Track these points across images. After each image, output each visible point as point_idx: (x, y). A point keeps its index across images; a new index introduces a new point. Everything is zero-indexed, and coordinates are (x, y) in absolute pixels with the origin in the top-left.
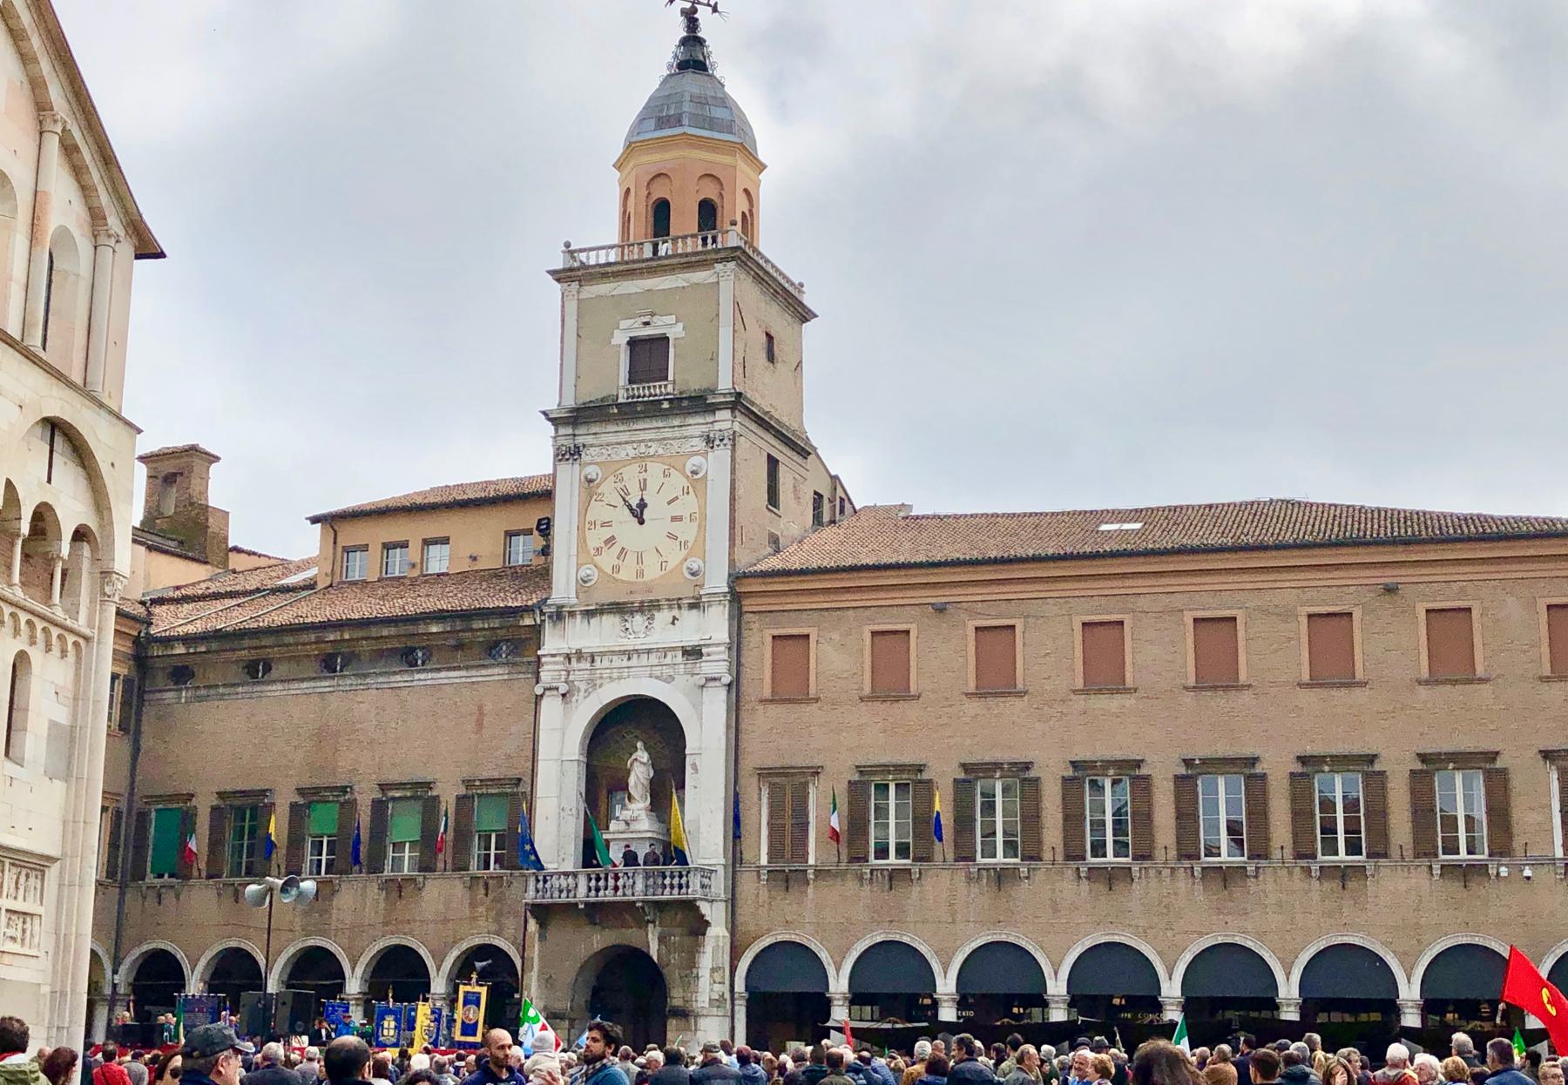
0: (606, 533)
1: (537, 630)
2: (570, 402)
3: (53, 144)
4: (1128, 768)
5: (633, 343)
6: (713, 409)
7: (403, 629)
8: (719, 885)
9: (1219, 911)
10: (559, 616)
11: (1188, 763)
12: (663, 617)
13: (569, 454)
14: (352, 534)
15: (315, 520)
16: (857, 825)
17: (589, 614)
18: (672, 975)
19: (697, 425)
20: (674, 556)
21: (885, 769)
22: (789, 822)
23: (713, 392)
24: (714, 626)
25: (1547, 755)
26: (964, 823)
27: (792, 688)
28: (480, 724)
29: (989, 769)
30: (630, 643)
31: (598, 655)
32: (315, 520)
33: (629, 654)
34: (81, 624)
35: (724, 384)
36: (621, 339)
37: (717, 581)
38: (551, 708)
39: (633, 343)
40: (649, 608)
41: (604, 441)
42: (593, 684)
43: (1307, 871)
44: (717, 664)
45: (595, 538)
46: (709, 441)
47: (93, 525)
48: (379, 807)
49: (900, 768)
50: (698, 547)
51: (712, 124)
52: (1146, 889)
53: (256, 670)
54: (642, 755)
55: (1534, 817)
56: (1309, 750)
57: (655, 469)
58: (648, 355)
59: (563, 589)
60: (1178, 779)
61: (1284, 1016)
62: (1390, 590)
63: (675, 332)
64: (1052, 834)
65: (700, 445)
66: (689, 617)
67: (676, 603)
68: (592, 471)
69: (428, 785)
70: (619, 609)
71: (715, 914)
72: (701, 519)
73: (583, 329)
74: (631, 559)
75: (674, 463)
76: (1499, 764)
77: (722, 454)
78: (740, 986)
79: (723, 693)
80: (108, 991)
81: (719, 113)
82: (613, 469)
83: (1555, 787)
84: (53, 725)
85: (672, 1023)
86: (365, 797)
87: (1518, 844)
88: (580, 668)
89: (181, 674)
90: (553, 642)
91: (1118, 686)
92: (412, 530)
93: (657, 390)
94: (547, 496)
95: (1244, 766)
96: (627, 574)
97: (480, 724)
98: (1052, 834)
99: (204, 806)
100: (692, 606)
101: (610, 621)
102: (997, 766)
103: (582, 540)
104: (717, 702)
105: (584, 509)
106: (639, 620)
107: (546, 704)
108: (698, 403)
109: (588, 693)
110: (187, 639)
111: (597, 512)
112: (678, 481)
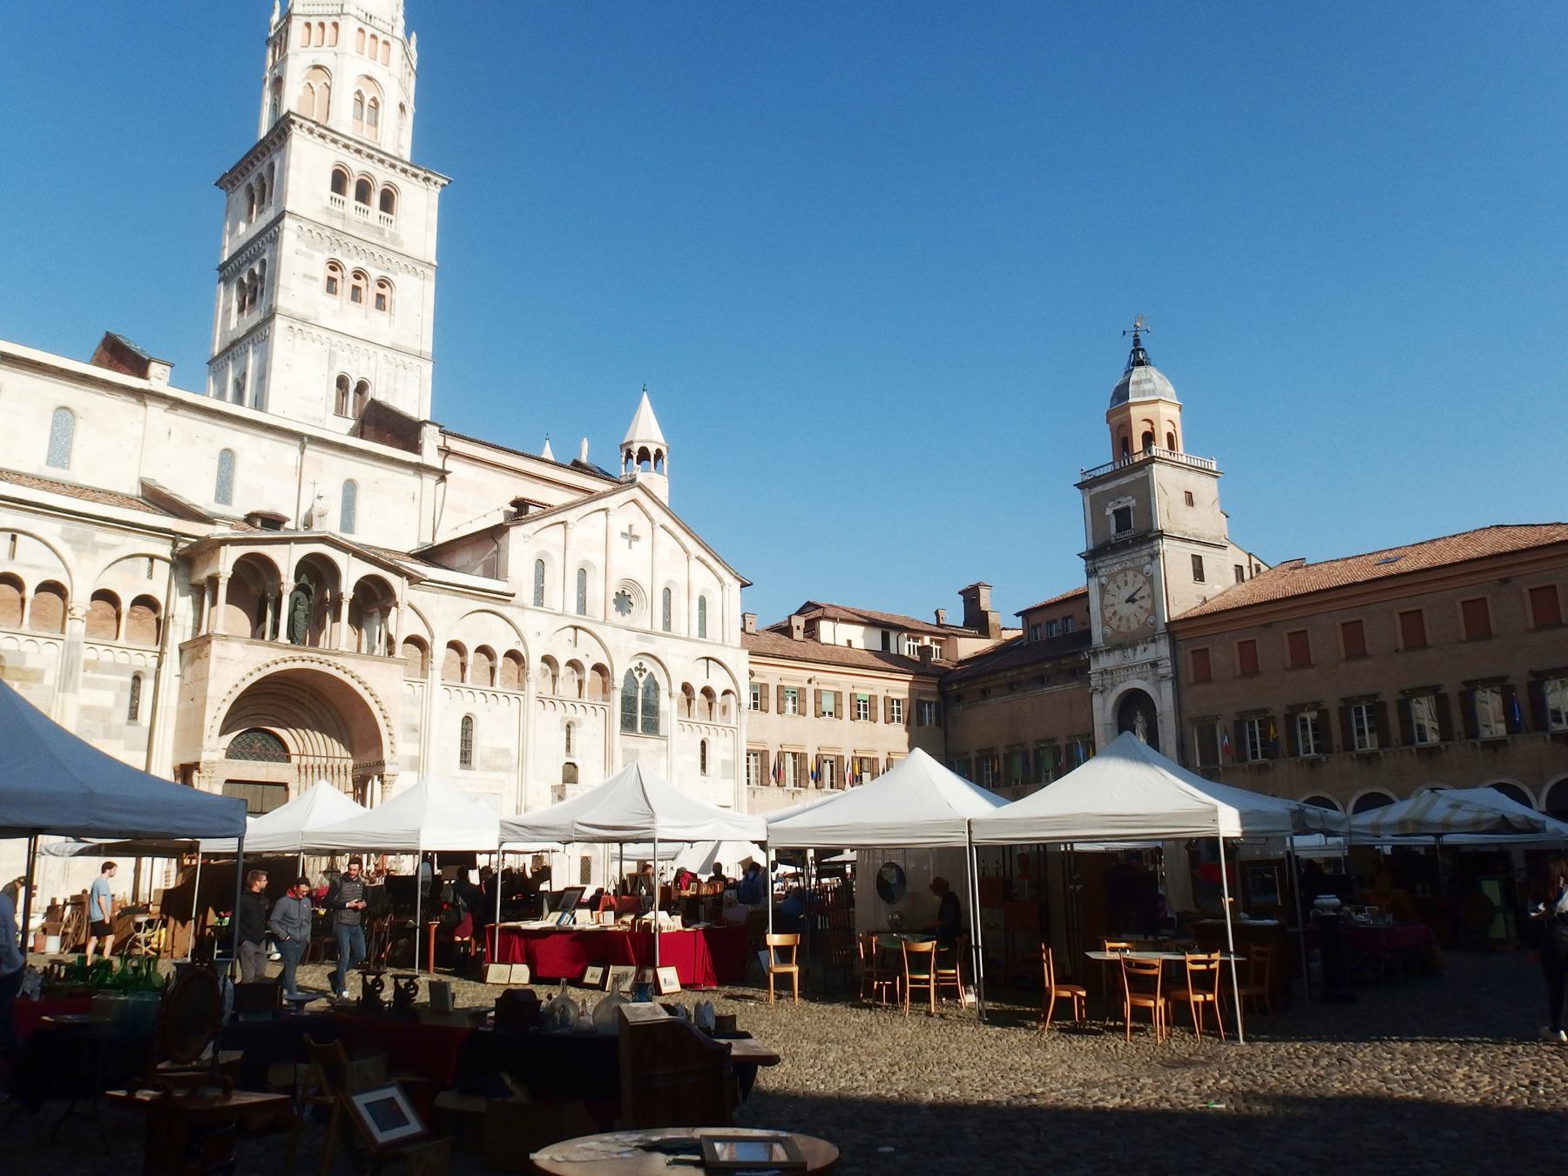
0: (1112, 610)
2: (1091, 547)
3: (695, 563)
4: (1316, 705)
5: (1115, 512)
10: (1096, 654)
11: (1403, 692)
12: (1140, 648)
13: (1091, 573)
14: (1035, 619)
15: (1017, 615)
16: (1239, 740)
17: (1108, 651)
20: (1143, 617)
21: (1250, 712)
23: (1151, 531)
24: (1163, 649)
26: (1292, 736)
27: (1203, 675)
29: (1303, 707)
30: (1128, 662)
32: (1017, 615)
33: (1127, 669)
34: (733, 724)
36: (1109, 512)
38: (1097, 700)
39: (1115, 512)
40: (1133, 645)
41: (1110, 565)
42: (1113, 685)
43: (1474, 745)
44: (1166, 668)
45: (1108, 614)
47: (733, 688)
48: (1036, 752)
49: (1257, 712)
51: (1144, 393)
53: (985, 693)
54: (1140, 718)
56: (1469, 677)
57: (1130, 574)
58: (1122, 516)
60: (1399, 702)
62: (1504, 581)
63: (1132, 503)
64: (1337, 739)
65: (1147, 559)
66: (1152, 647)
68: (1104, 580)
69: (1053, 740)
70: (1121, 647)
73: (1096, 509)
74: (1124, 621)
75: (1139, 570)
79: (1170, 684)
81: (1147, 386)
82: (1112, 577)
84: (724, 761)
86: (1031, 747)
88: (1108, 680)
89: (959, 698)
90: (1094, 667)
91: (1363, 655)
92: (1057, 614)
93: (1127, 533)
94: (1085, 595)
95: (1434, 691)
98: (1337, 739)
99: (973, 756)
100: (1154, 641)
101: (1118, 653)
102: (1305, 705)
105: (1102, 599)
107: (1095, 697)
111: (1109, 599)
112: (1141, 578)
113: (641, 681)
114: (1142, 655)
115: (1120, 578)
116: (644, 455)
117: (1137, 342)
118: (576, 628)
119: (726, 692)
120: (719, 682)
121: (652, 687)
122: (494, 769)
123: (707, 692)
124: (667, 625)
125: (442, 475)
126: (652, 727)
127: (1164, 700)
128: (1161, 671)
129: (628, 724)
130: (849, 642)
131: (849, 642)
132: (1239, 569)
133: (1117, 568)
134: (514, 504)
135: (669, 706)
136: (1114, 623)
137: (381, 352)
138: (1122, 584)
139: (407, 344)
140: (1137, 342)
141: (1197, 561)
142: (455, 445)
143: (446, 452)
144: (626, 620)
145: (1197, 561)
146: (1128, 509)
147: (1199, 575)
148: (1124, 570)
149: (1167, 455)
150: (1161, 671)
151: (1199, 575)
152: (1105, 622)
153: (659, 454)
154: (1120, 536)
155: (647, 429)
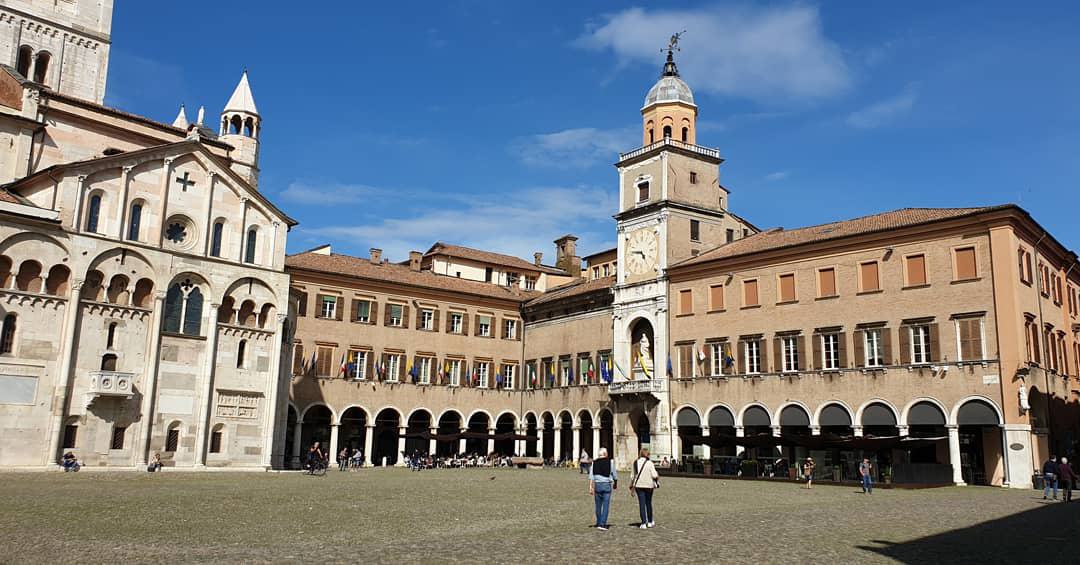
1: (613, 296)
6: (661, 207)
7: (581, 298)
8: (664, 386)
9: (830, 390)
10: (618, 289)
18: (650, 419)
19: (656, 215)
22: (686, 361)
25: (954, 317)
28: (601, 331)
31: (629, 306)
35: (665, 197)
36: (636, 185)
37: (661, 274)
39: (640, 186)
40: (643, 284)
46: (659, 220)
50: (657, 261)
51: (668, 97)
52: (805, 380)
55: (949, 344)
57: (645, 231)
59: (621, 281)
61: (775, 435)
67: (650, 282)
70: (634, 285)
71: (662, 397)
72: (657, 249)
76: (935, 321)
77: (664, 224)
78: (674, 423)
80: (518, 426)
82: (633, 233)
83: (958, 330)
85: (651, 437)
87: (942, 357)
90: (618, 299)
96: (638, 273)
97: (601, 331)
103: (626, 261)
104: (662, 316)
106: (640, 288)
108: (655, 207)
109: (627, 317)
110: (533, 307)
113: (186, 294)
114: (648, 292)
115: (638, 235)
116: (236, 120)
117: (670, 57)
118: (125, 252)
119: (267, 306)
120: (260, 297)
121: (196, 299)
122: (34, 357)
123: (248, 305)
124: (216, 250)
125: (38, 132)
126: (193, 330)
127: (659, 325)
128: (659, 306)
129: (168, 328)
130: (458, 274)
131: (458, 274)
132: (730, 232)
133: (638, 226)
134: (106, 152)
135: (209, 314)
136: (632, 268)
137: (62, 32)
138: (639, 239)
139: (88, 27)
140: (670, 57)
141: (695, 224)
142: (53, 104)
143: (42, 110)
144: (177, 246)
145: (695, 224)
146: (647, 183)
147: (695, 235)
148: (643, 228)
149: (681, 146)
150: (659, 306)
151: (695, 235)
152: (627, 267)
153: (249, 122)
154: (643, 205)
155: (242, 100)
